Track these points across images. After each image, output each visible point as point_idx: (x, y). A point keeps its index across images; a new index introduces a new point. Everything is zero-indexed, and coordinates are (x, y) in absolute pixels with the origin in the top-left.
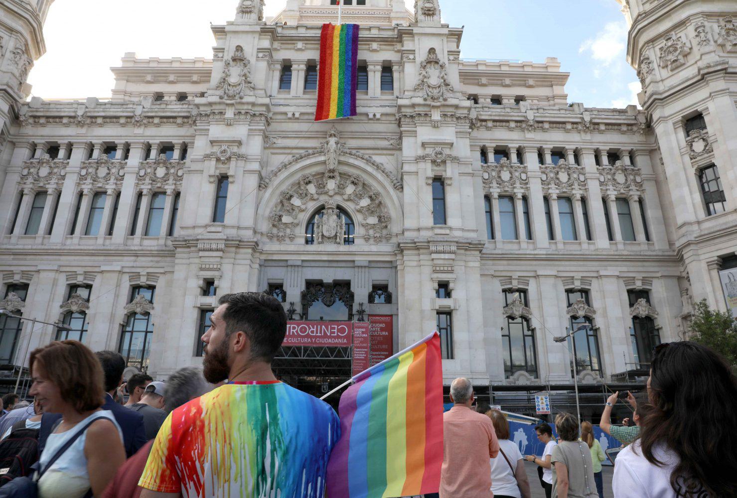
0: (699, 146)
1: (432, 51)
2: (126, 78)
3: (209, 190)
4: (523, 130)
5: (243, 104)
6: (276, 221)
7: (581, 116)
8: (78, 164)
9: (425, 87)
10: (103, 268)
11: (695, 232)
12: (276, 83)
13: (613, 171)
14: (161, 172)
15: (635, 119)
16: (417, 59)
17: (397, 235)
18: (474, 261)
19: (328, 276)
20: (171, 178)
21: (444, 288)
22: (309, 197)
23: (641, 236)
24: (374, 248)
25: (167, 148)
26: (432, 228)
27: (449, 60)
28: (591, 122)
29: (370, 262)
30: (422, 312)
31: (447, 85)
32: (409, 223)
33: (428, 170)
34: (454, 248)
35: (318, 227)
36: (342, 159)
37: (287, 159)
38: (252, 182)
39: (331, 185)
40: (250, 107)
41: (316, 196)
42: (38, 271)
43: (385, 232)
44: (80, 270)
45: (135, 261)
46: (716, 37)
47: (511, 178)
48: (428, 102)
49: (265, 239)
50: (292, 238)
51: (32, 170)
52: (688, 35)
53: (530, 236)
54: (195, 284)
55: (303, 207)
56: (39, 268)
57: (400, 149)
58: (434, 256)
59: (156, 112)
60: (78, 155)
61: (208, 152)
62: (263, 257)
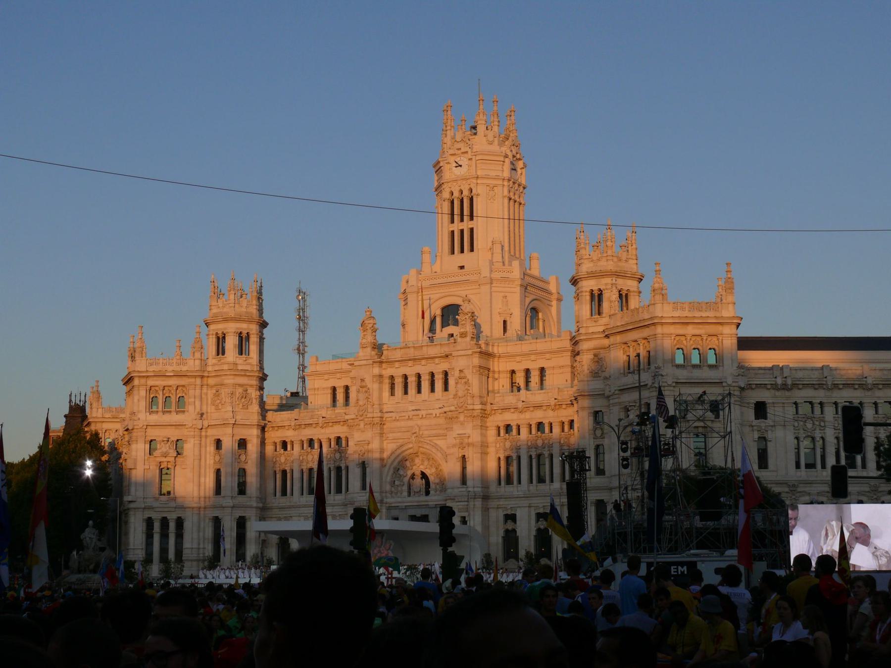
1: (461, 371)
7: (549, 401)
12: (386, 393)
18: (479, 503)
20: (343, 459)
24: (436, 498)
25: (338, 439)
26: (459, 488)
27: (473, 372)
34: (466, 499)
40: (371, 419)
42: (291, 517)
45: (333, 509)
48: (458, 409)
49: (388, 495)
55: (405, 474)
56: (292, 515)
58: (458, 504)
60: (297, 447)
62: (387, 505)
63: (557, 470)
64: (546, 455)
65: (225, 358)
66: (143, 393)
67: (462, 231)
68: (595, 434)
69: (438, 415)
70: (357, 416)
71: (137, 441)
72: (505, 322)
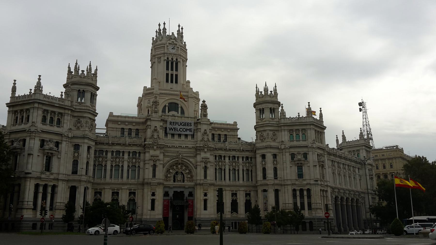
0: (264, 163)
2: (112, 122)
3: (151, 169)
4: (226, 151)
5: (158, 144)
6: (166, 176)
8: (110, 157)
9: (203, 141)
10: (122, 188)
11: (259, 183)
13: (246, 163)
14: (134, 160)
15: (253, 149)
16: (201, 131)
17: (195, 180)
19: (179, 190)
20: (137, 162)
21: (205, 195)
22: (174, 169)
23: (250, 180)
24: (190, 183)
26: (204, 180)
28: (242, 150)
29: (189, 187)
30: (201, 200)
31: (209, 140)
32: (198, 178)
33: (203, 165)
34: (208, 185)
35: (176, 178)
36: (182, 160)
37: (167, 159)
38: (162, 166)
39: (179, 166)
41: (176, 169)
42: (104, 189)
43: (192, 179)
44: (116, 188)
46: (271, 136)
47: (222, 164)
48: (204, 146)
50: (170, 181)
51: (97, 159)
52: (265, 134)
53: (225, 180)
54: (150, 194)
57: (196, 157)
58: (204, 187)
59: (132, 143)
60: (109, 155)
61: (150, 158)
63: (241, 176)
64: (237, 170)
65: (84, 104)
66: (40, 112)
67: (172, 75)
68: (274, 163)
69: (191, 147)
70: (153, 143)
71: (35, 139)
72: (196, 114)
